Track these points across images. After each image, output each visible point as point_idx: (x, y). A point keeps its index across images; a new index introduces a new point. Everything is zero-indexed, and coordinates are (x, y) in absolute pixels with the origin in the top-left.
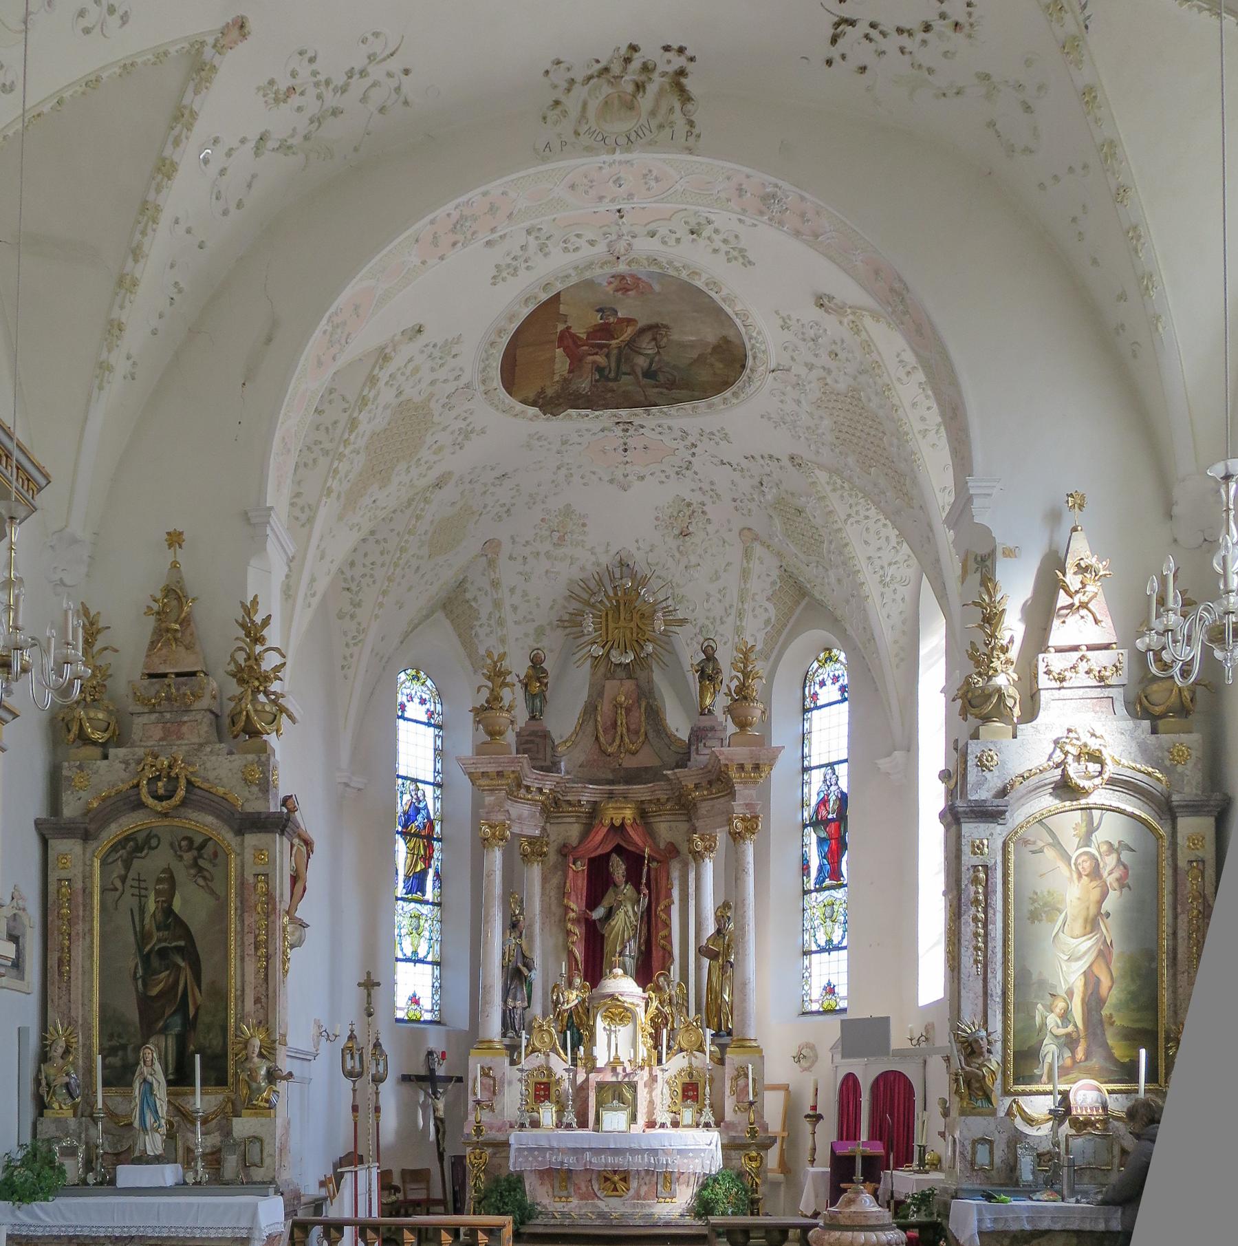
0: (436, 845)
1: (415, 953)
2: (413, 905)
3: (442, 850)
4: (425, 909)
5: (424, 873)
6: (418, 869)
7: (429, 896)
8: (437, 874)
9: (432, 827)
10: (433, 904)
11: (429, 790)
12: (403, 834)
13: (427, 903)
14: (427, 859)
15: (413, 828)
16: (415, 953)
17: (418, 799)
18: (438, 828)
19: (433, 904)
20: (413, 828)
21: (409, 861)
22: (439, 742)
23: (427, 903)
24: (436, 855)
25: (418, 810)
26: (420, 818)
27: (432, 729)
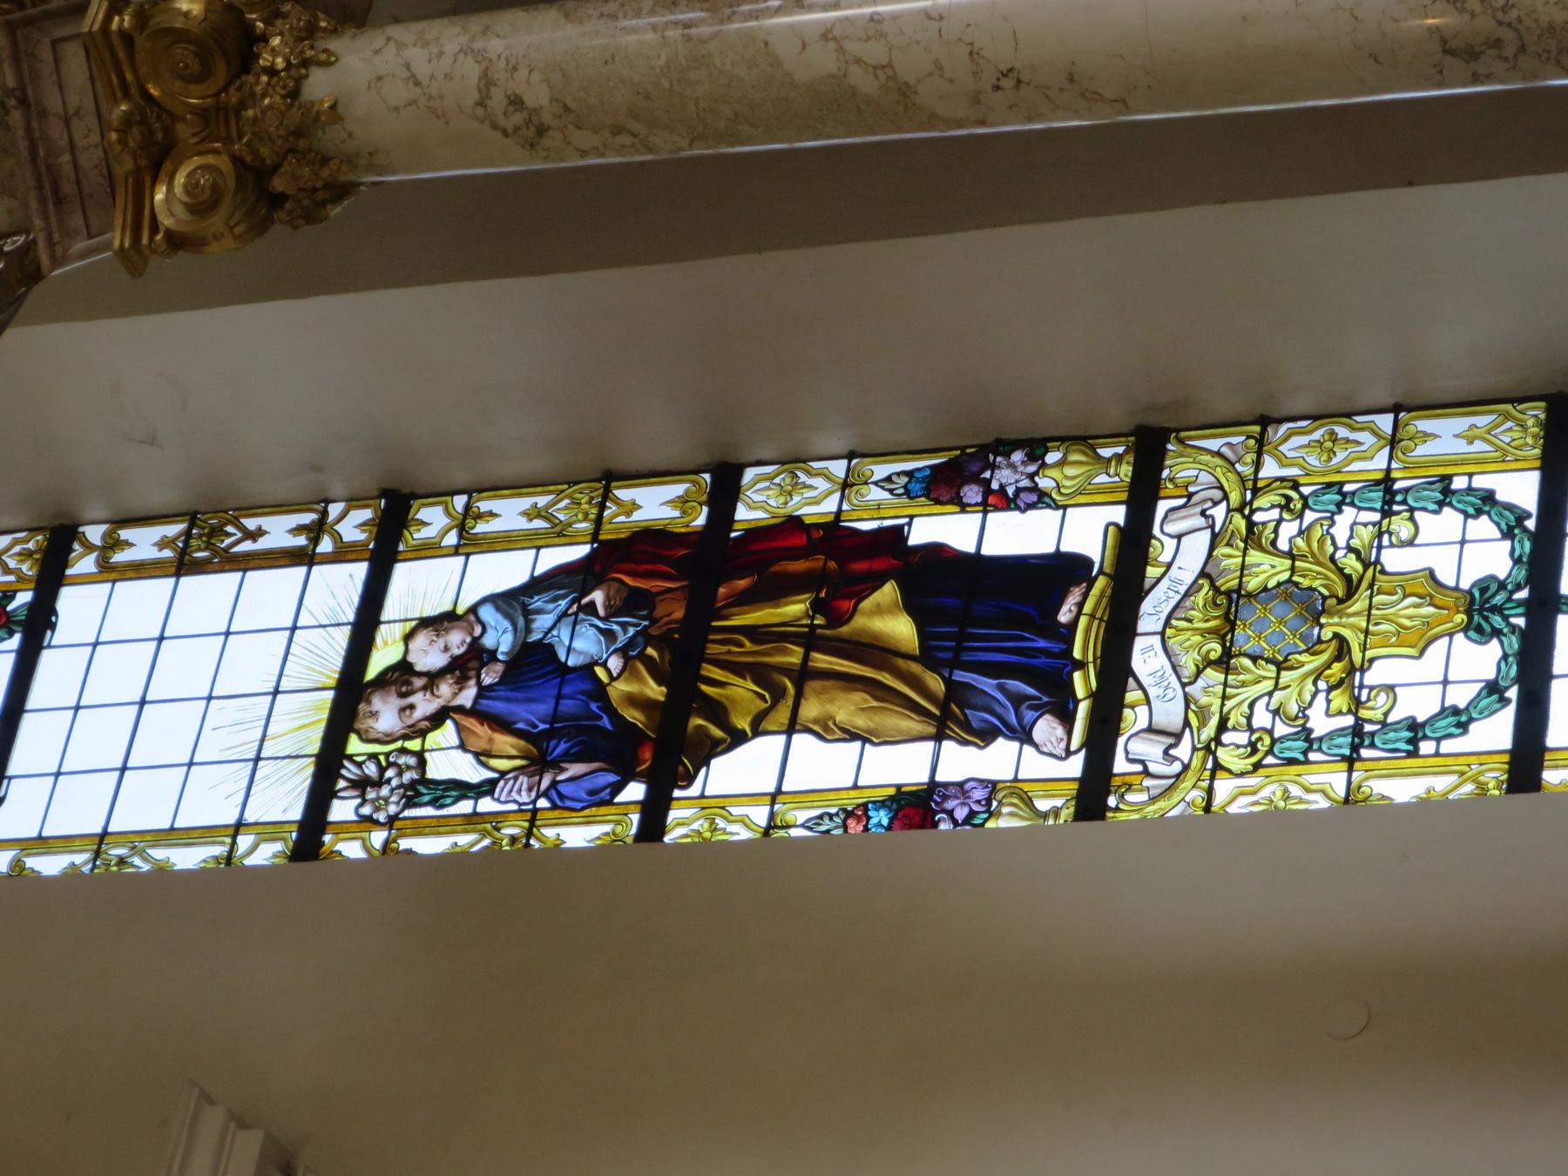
0: (755, 507)
1: (1478, 609)
2: (1146, 659)
3: (794, 460)
4: (1181, 551)
5: (939, 581)
6: (901, 629)
7: (1087, 531)
8: (942, 487)
9: (650, 544)
10: (1142, 496)
11: (419, 587)
12: (670, 750)
13: (1133, 543)
14: (846, 560)
15: (634, 689)
16: (1478, 609)
17: (463, 666)
18: (653, 505)
19: (1142, 496)
20: (634, 689)
21: (847, 708)
22: (144, 543)
23: (1133, 543)
24: (817, 501)
25: (534, 662)
26: (582, 644)
27: (70, 602)
